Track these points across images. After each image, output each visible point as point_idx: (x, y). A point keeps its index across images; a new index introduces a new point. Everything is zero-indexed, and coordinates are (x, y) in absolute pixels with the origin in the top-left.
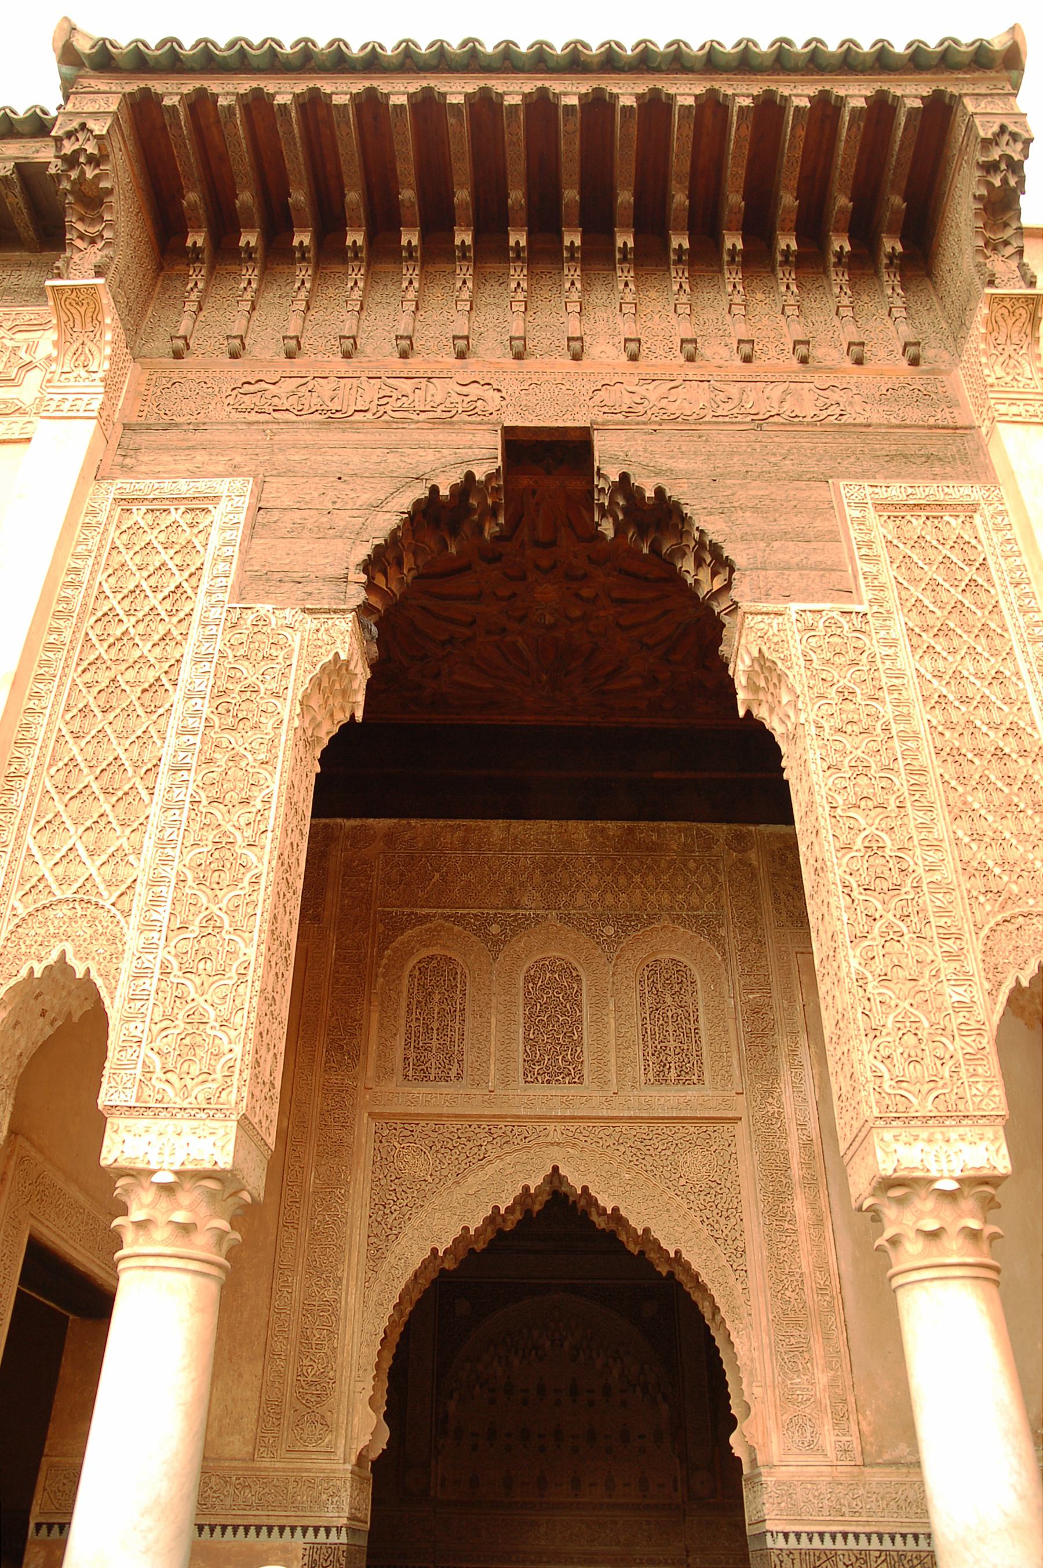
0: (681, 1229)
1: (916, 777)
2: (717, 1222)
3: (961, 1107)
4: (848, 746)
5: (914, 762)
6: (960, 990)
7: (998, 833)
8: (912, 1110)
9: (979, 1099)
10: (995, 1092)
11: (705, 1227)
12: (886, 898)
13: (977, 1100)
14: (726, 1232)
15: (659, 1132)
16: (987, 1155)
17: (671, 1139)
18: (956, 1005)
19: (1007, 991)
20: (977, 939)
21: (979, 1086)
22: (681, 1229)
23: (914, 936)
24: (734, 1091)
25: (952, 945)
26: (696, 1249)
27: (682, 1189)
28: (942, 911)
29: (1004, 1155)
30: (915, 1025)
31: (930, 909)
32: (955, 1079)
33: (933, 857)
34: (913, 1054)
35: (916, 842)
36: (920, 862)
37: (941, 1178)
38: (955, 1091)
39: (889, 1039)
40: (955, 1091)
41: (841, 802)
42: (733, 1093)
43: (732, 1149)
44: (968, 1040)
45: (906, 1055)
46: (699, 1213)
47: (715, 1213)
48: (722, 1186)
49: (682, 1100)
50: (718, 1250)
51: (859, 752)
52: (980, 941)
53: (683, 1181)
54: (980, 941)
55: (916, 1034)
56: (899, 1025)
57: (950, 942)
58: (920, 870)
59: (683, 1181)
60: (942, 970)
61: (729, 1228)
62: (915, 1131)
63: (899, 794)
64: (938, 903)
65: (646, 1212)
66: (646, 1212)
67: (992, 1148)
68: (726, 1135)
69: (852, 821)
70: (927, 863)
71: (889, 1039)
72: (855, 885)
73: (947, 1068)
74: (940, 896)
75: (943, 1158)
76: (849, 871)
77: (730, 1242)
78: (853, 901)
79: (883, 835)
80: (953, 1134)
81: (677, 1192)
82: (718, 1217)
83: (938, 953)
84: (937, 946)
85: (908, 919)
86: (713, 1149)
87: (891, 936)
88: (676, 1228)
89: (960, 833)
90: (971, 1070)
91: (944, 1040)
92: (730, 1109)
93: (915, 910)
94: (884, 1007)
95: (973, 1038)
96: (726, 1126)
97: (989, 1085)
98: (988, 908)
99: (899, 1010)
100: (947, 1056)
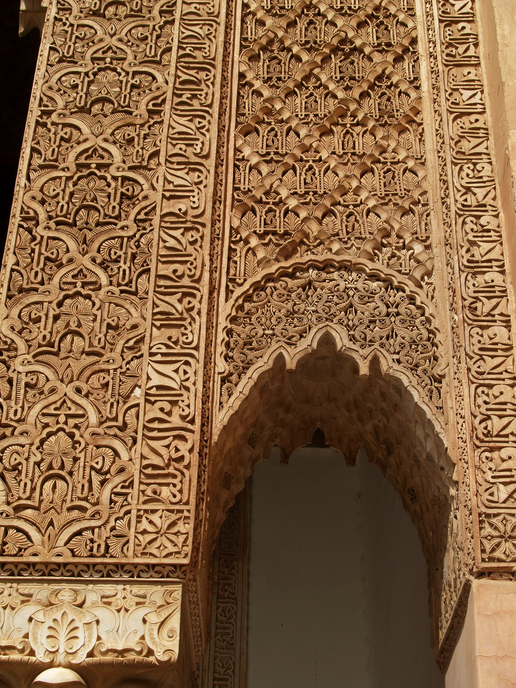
1: (192, 72)
3: (115, 550)
4: (100, 32)
5: (197, 53)
6: (168, 369)
7: (311, 153)
8: (30, 551)
9: (149, 537)
10: (181, 527)
12: (90, 235)
13: (145, 539)
16: (142, 629)
18: (153, 391)
19: (255, 376)
20: (227, 300)
21: (155, 518)
23: (116, 290)
25: (174, 304)
28: (174, 255)
29: (172, 631)
30: (72, 422)
31: (154, 250)
32: (117, 507)
33: (182, 178)
34: (56, 465)
35: (162, 160)
36: (159, 186)
37: (51, 665)
38: (112, 523)
39: (22, 440)
40: (112, 523)
41: (61, 103)
44: (156, 445)
45: (44, 466)
51: (114, 42)
52: (231, 302)
54: (231, 302)
55: (71, 435)
56: (45, 420)
57: (173, 300)
58: (156, 197)
60: (147, 339)
62: (25, 588)
63: (157, 94)
64: (171, 243)
67: (154, 619)
69: (68, 130)
70: (171, 187)
71: (22, 440)
72: (42, 216)
73: (109, 487)
74: (177, 233)
75: (63, 635)
76: (39, 196)
78: (34, 239)
79: (113, 149)
80: (92, 594)
83: (149, 317)
84: (150, 303)
85: (115, 267)
87: (79, 289)
89: (247, 152)
90: (149, 492)
91: (117, 444)
93: (130, 251)
94: (31, 392)
95: (166, 442)
97: (174, 517)
98: (261, 254)
99: (53, 398)
100: (113, 471)
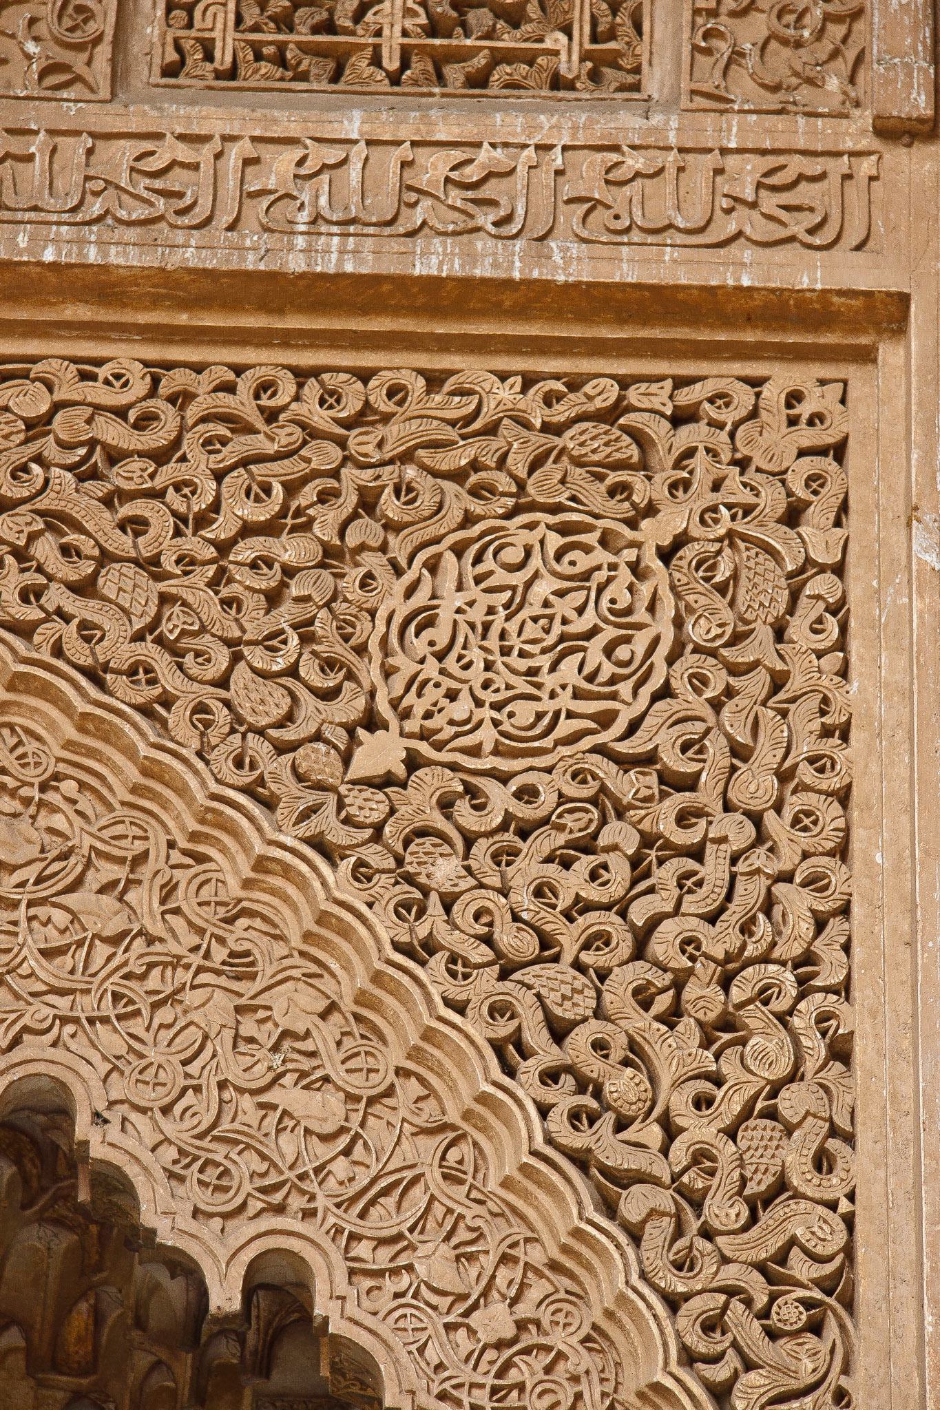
0: (323, 1109)
2: (636, 1055)
11: (528, 1085)
14: (699, 1130)
15: (243, 403)
17: (324, 455)
22: (323, 1109)
24: (864, 119)
26: (433, 1262)
27: (370, 806)
42: (856, 132)
43: (817, 538)
46: (486, 984)
47: (618, 993)
48: (707, 796)
49: (434, 167)
50: (614, 1275)
53: (381, 752)
59: (381, 752)
61: (730, 1105)
65: (49, 972)
66: (49, 972)
68: (774, 442)
77: (724, 1210)
81: (328, 824)
82: (640, 1022)
86: (656, 533)
88: (287, 1096)
92: (822, 237)
96: (783, 377)
